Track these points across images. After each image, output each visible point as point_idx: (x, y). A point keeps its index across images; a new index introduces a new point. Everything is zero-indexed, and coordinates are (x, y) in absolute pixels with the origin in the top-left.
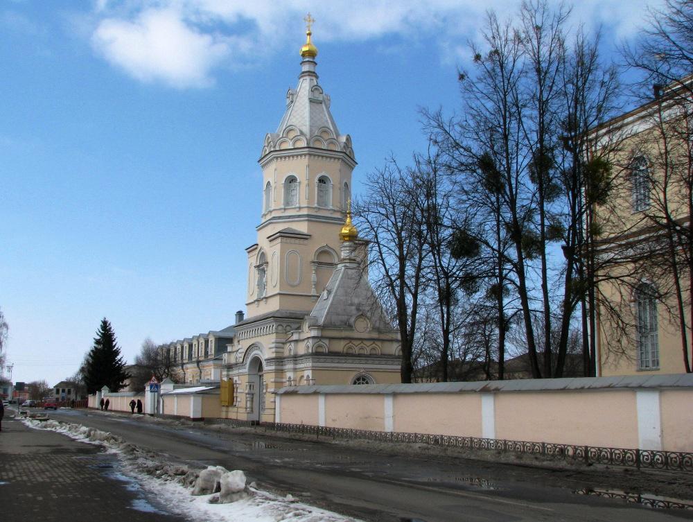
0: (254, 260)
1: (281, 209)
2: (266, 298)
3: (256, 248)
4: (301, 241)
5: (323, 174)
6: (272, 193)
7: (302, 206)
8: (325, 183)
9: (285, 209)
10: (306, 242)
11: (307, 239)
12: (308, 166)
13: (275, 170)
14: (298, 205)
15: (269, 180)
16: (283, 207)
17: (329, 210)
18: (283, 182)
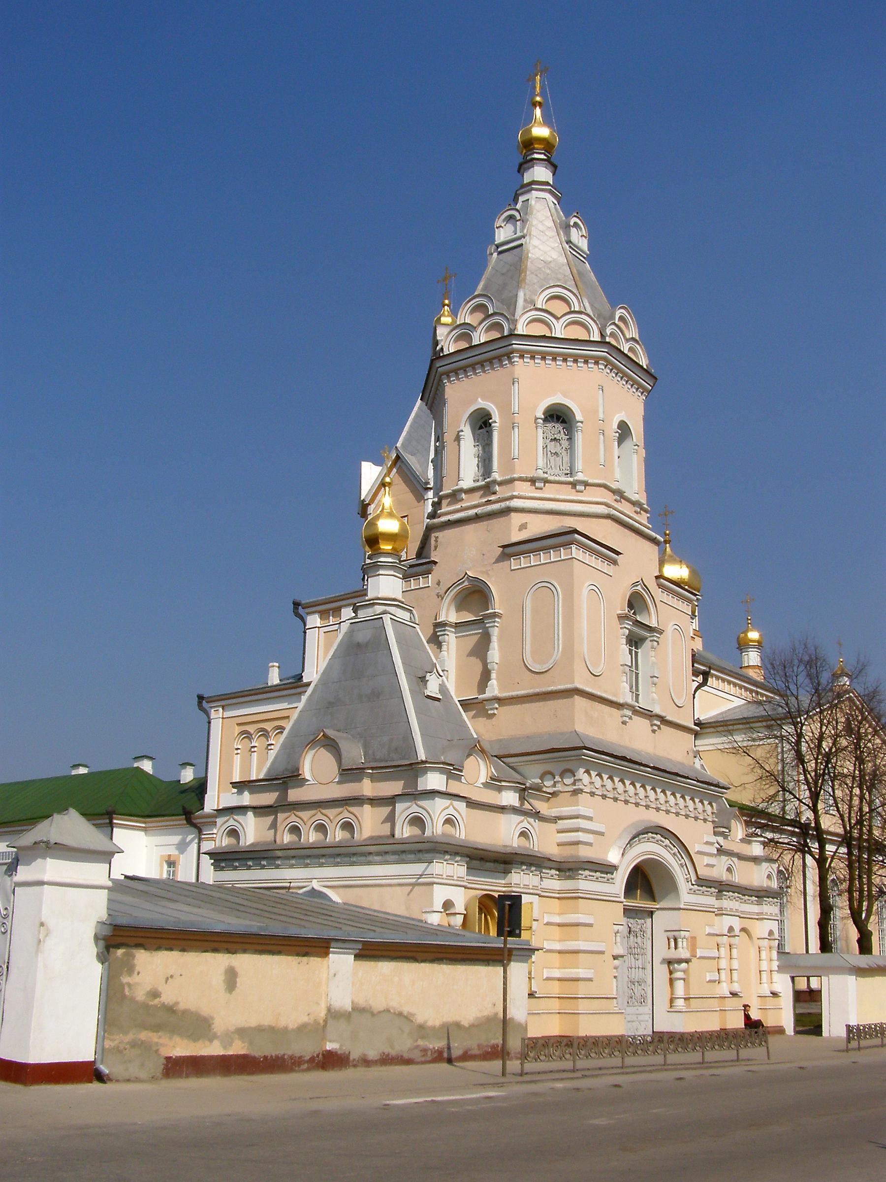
7: (590, 481)
15: (481, 403)
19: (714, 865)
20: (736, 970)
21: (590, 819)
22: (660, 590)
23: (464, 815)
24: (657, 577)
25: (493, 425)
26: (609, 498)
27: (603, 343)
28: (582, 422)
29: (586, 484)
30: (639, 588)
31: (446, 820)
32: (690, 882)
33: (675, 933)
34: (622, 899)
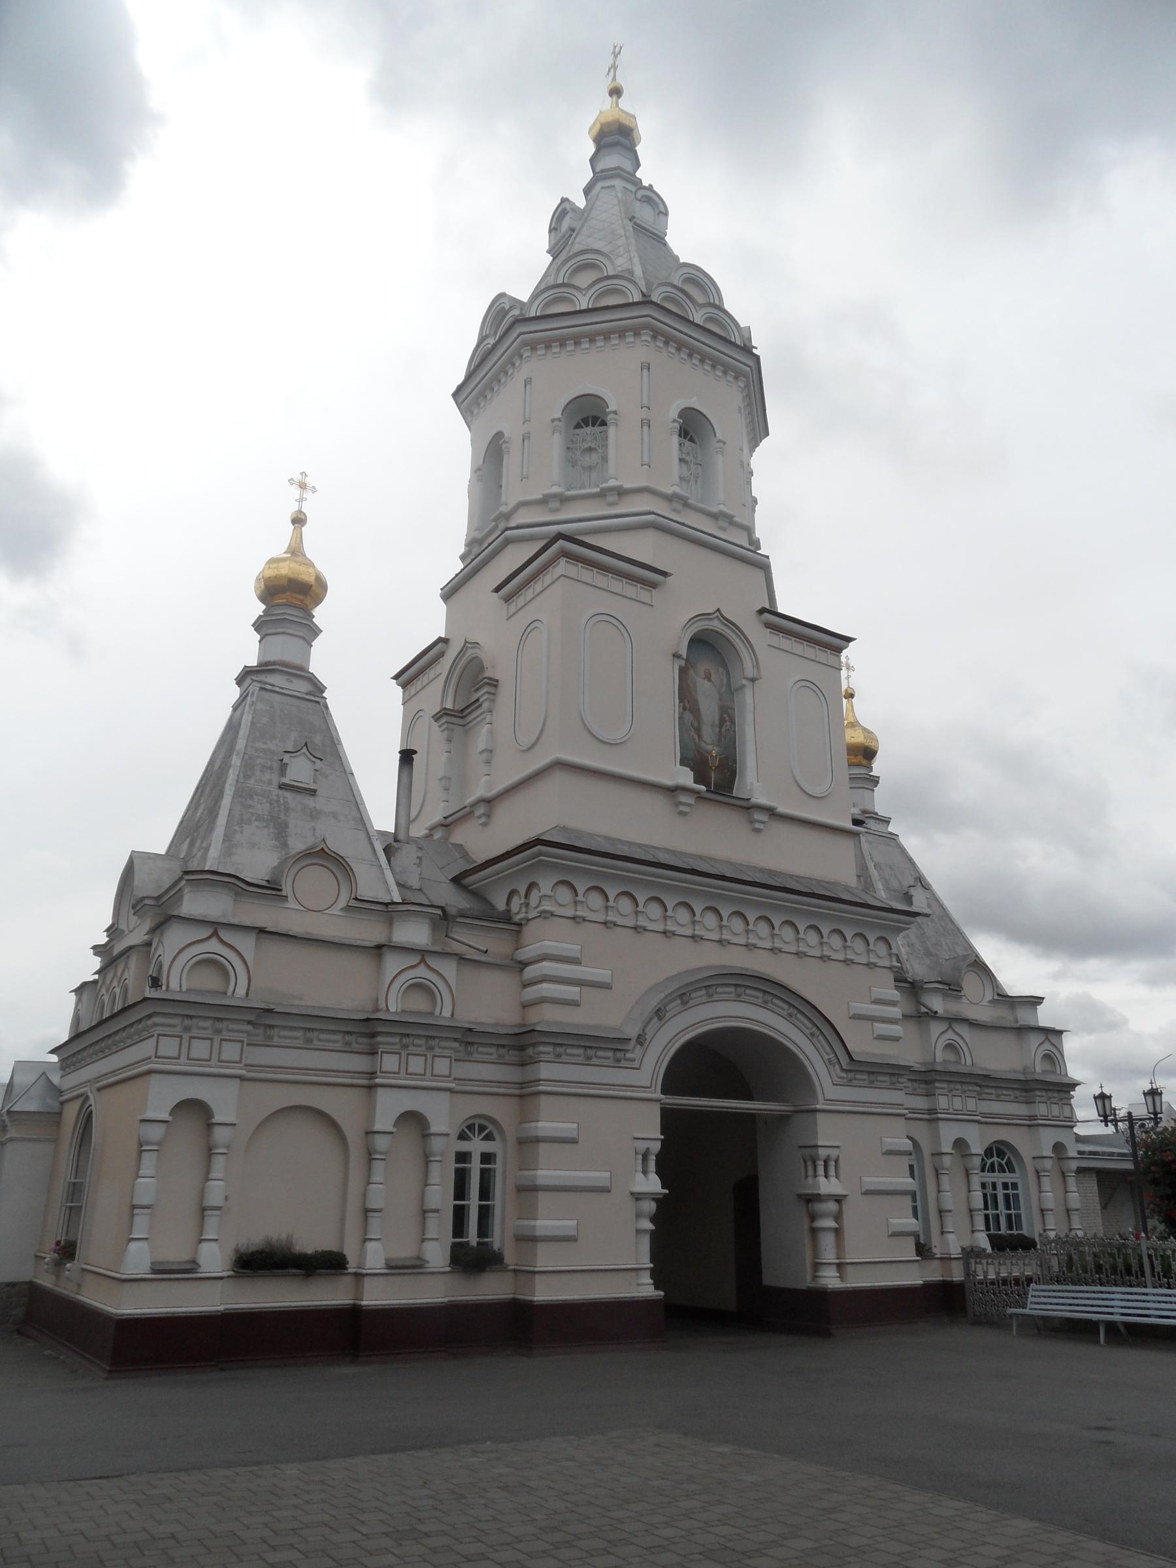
0: (434, 695)
1: (545, 501)
2: (488, 802)
3: (442, 654)
4: (631, 590)
5: (694, 403)
6: (512, 463)
7: (628, 485)
8: (692, 440)
9: (564, 500)
10: (644, 594)
11: (653, 585)
12: (646, 367)
13: (528, 382)
14: (612, 483)
16: (556, 489)
17: (715, 517)
18: (558, 415)
19: (900, 1038)
20: (1052, 1210)
21: (575, 961)
22: (769, 630)
23: (452, 981)
24: (762, 611)
25: (504, 446)
26: (662, 508)
27: (647, 302)
28: (615, 412)
29: (621, 492)
30: (716, 625)
31: (946, 1045)
32: (837, 1067)
33: (807, 1152)
34: (658, 1095)
